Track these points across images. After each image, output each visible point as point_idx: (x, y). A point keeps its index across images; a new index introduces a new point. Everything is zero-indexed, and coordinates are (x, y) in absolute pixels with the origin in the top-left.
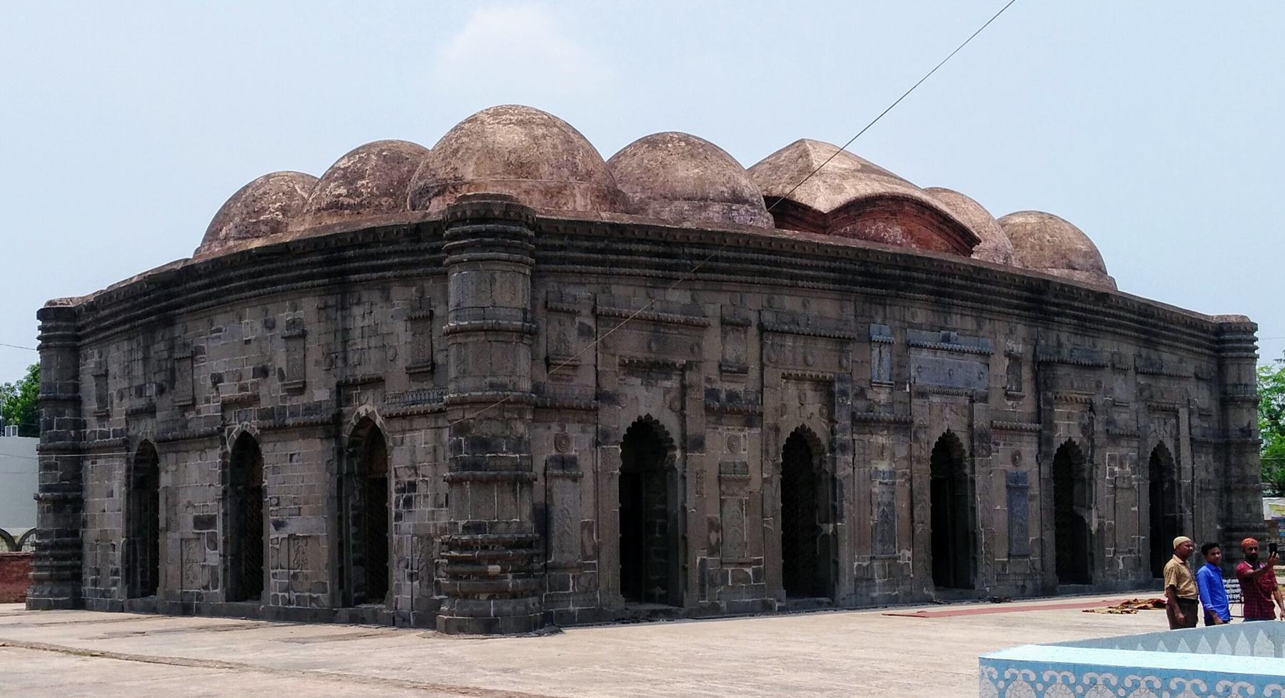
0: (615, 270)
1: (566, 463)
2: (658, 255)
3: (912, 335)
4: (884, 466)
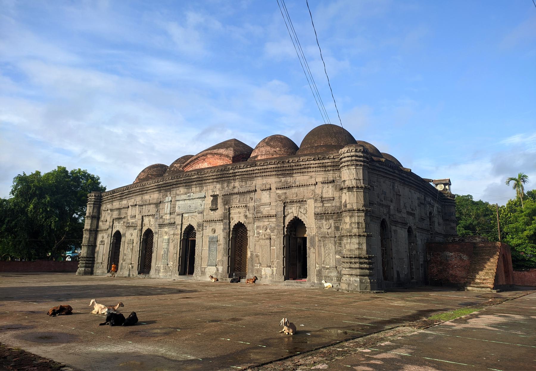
3: (178, 198)
4: (166, 237)
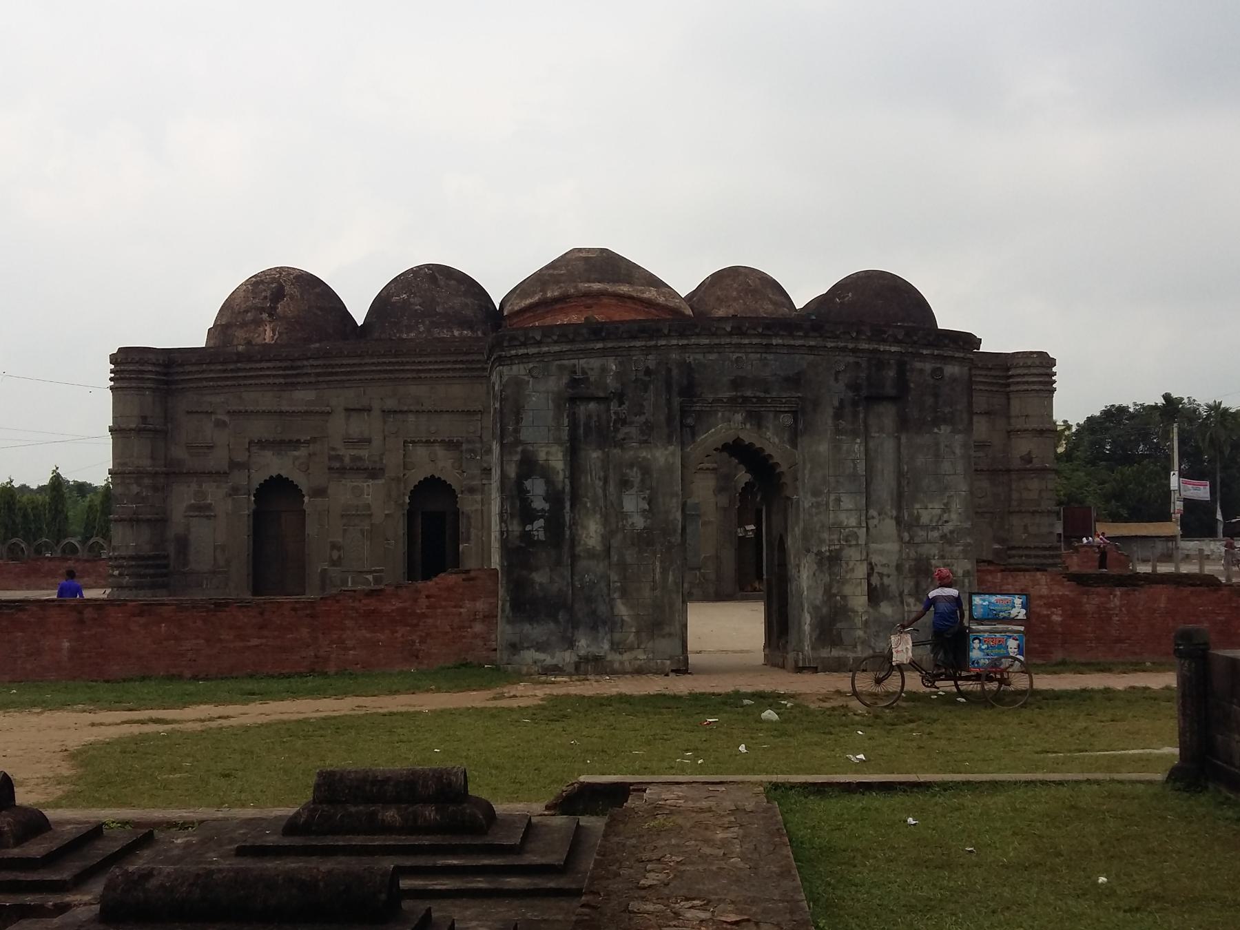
0: (242, 382)
1: (202, 510)
2: (280, 368)
